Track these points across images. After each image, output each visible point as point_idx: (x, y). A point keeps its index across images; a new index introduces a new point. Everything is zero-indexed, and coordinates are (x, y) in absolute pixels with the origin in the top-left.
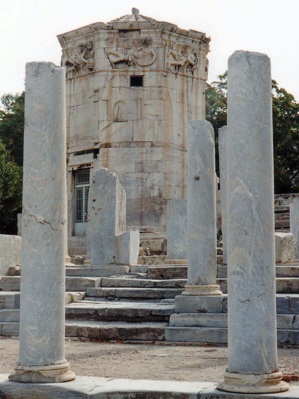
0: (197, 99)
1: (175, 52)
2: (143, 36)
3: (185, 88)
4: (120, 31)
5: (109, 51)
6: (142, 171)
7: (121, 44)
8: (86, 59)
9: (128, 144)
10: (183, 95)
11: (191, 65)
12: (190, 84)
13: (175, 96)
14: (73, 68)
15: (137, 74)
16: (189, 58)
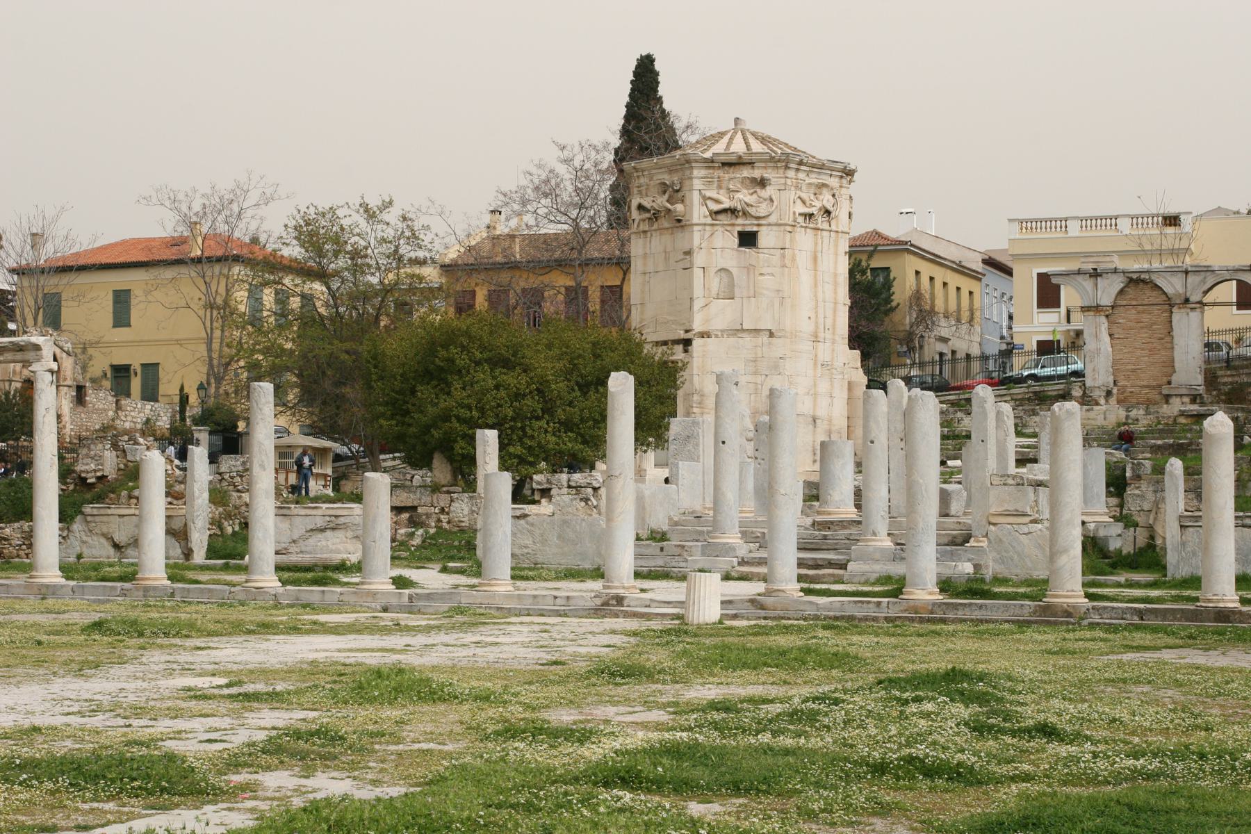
0: (836, 263)
1: (804, 195)
2: (757, 174)
3: (819, 248)
4: (724, 164)
5: (708, 194)
6: (755, 373)
7: (724, 185)
8: (672, 204)
9: (739, 331)
10: (815, 259)
11: (828, 212)
12: (826, 241)
13: (803, 260)
14: (647, 215)
15: (748, 229)
16: (825, 203)
